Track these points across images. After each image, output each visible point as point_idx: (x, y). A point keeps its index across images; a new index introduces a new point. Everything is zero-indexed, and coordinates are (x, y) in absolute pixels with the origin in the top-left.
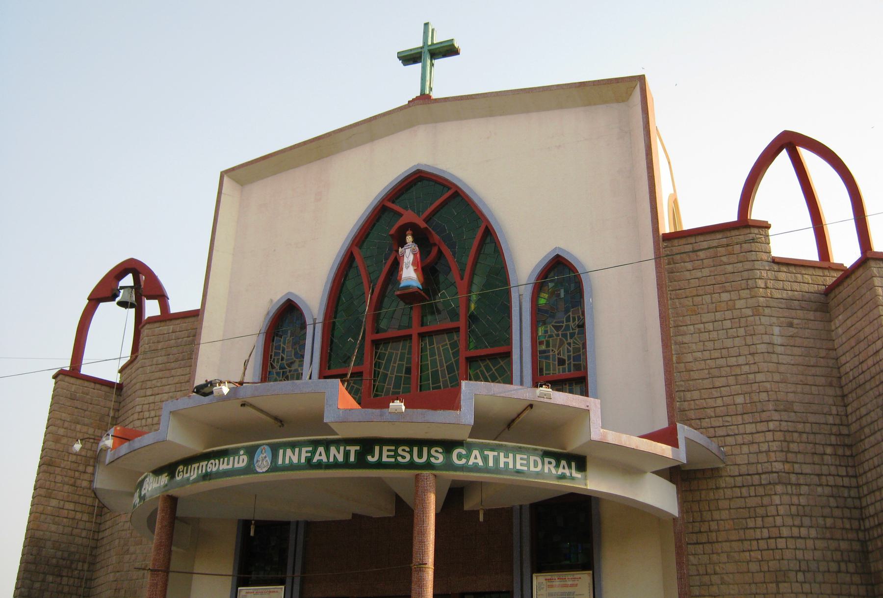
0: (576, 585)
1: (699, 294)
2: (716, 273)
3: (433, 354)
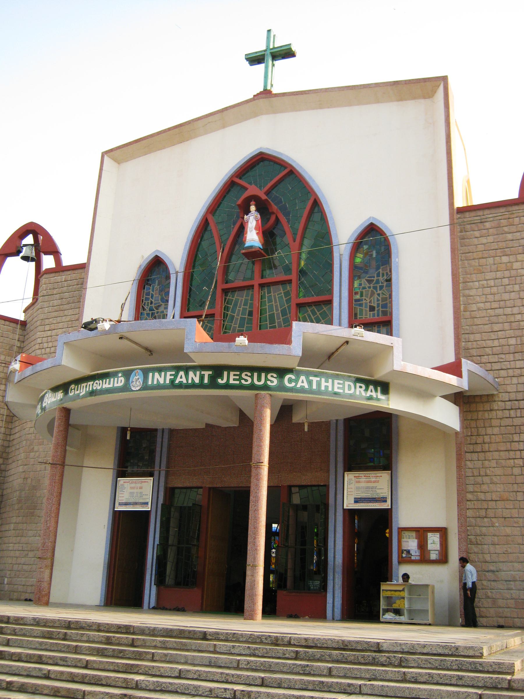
0: (378, 482)
1: (484, 257)
2: (498, 240)
3: (270, 301)
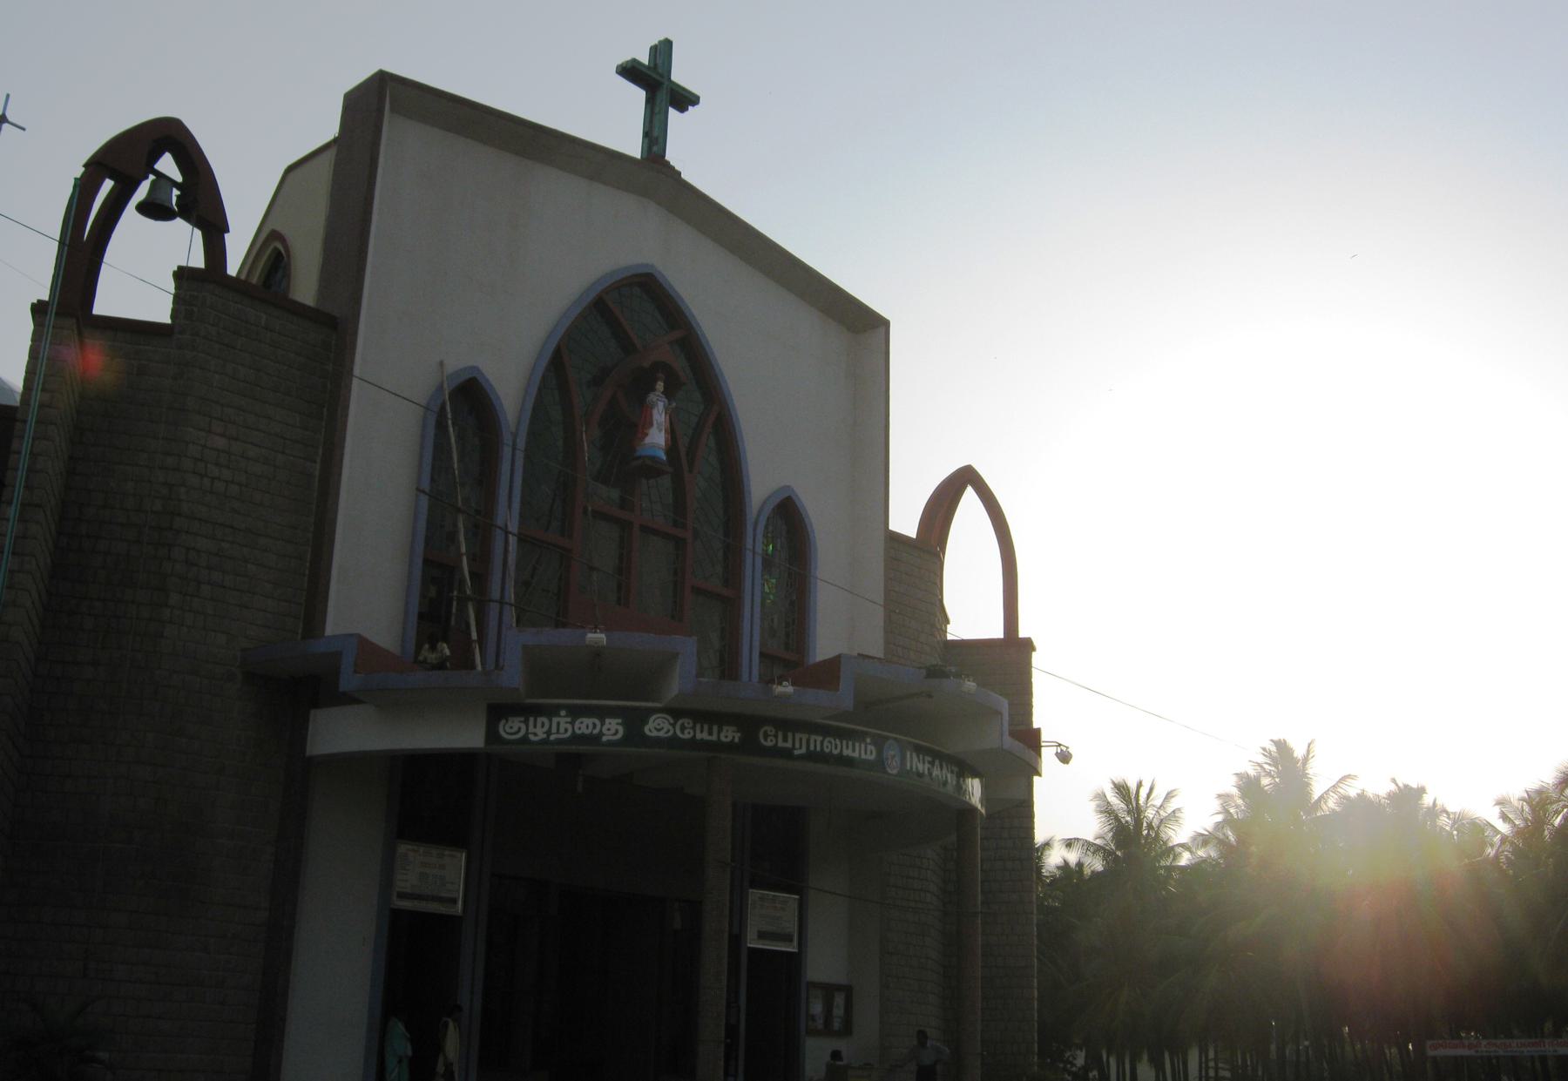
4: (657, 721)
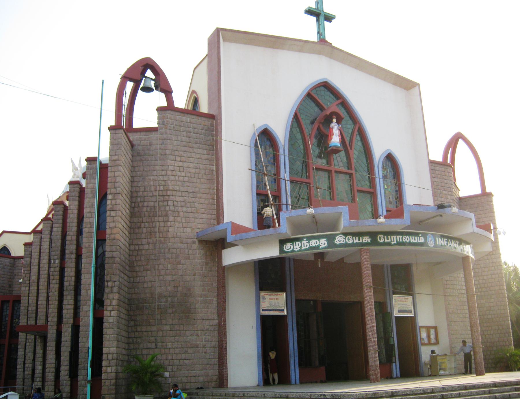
0: (407, 301)
4: (339, 238)
